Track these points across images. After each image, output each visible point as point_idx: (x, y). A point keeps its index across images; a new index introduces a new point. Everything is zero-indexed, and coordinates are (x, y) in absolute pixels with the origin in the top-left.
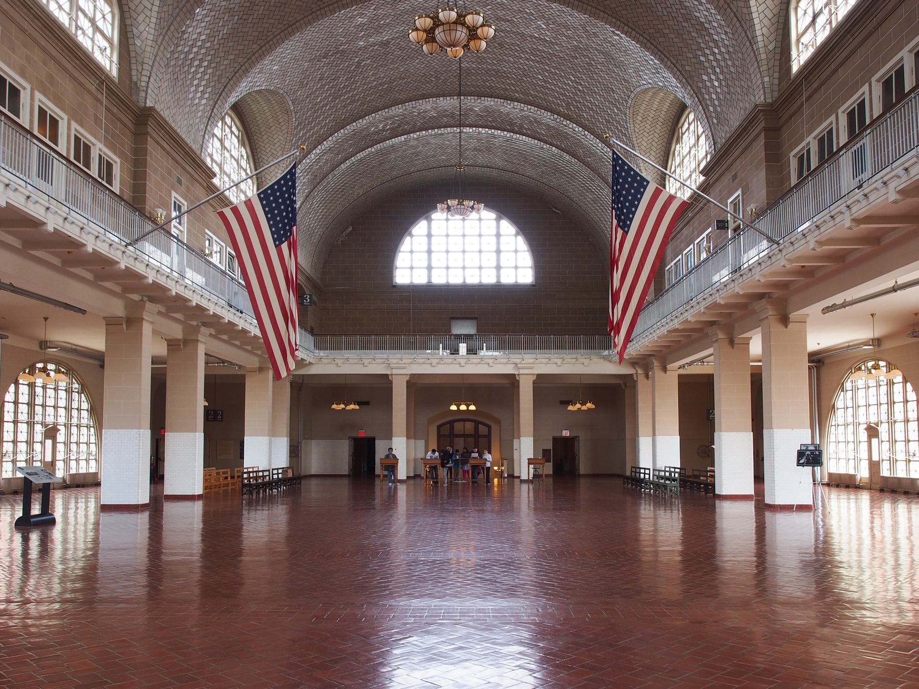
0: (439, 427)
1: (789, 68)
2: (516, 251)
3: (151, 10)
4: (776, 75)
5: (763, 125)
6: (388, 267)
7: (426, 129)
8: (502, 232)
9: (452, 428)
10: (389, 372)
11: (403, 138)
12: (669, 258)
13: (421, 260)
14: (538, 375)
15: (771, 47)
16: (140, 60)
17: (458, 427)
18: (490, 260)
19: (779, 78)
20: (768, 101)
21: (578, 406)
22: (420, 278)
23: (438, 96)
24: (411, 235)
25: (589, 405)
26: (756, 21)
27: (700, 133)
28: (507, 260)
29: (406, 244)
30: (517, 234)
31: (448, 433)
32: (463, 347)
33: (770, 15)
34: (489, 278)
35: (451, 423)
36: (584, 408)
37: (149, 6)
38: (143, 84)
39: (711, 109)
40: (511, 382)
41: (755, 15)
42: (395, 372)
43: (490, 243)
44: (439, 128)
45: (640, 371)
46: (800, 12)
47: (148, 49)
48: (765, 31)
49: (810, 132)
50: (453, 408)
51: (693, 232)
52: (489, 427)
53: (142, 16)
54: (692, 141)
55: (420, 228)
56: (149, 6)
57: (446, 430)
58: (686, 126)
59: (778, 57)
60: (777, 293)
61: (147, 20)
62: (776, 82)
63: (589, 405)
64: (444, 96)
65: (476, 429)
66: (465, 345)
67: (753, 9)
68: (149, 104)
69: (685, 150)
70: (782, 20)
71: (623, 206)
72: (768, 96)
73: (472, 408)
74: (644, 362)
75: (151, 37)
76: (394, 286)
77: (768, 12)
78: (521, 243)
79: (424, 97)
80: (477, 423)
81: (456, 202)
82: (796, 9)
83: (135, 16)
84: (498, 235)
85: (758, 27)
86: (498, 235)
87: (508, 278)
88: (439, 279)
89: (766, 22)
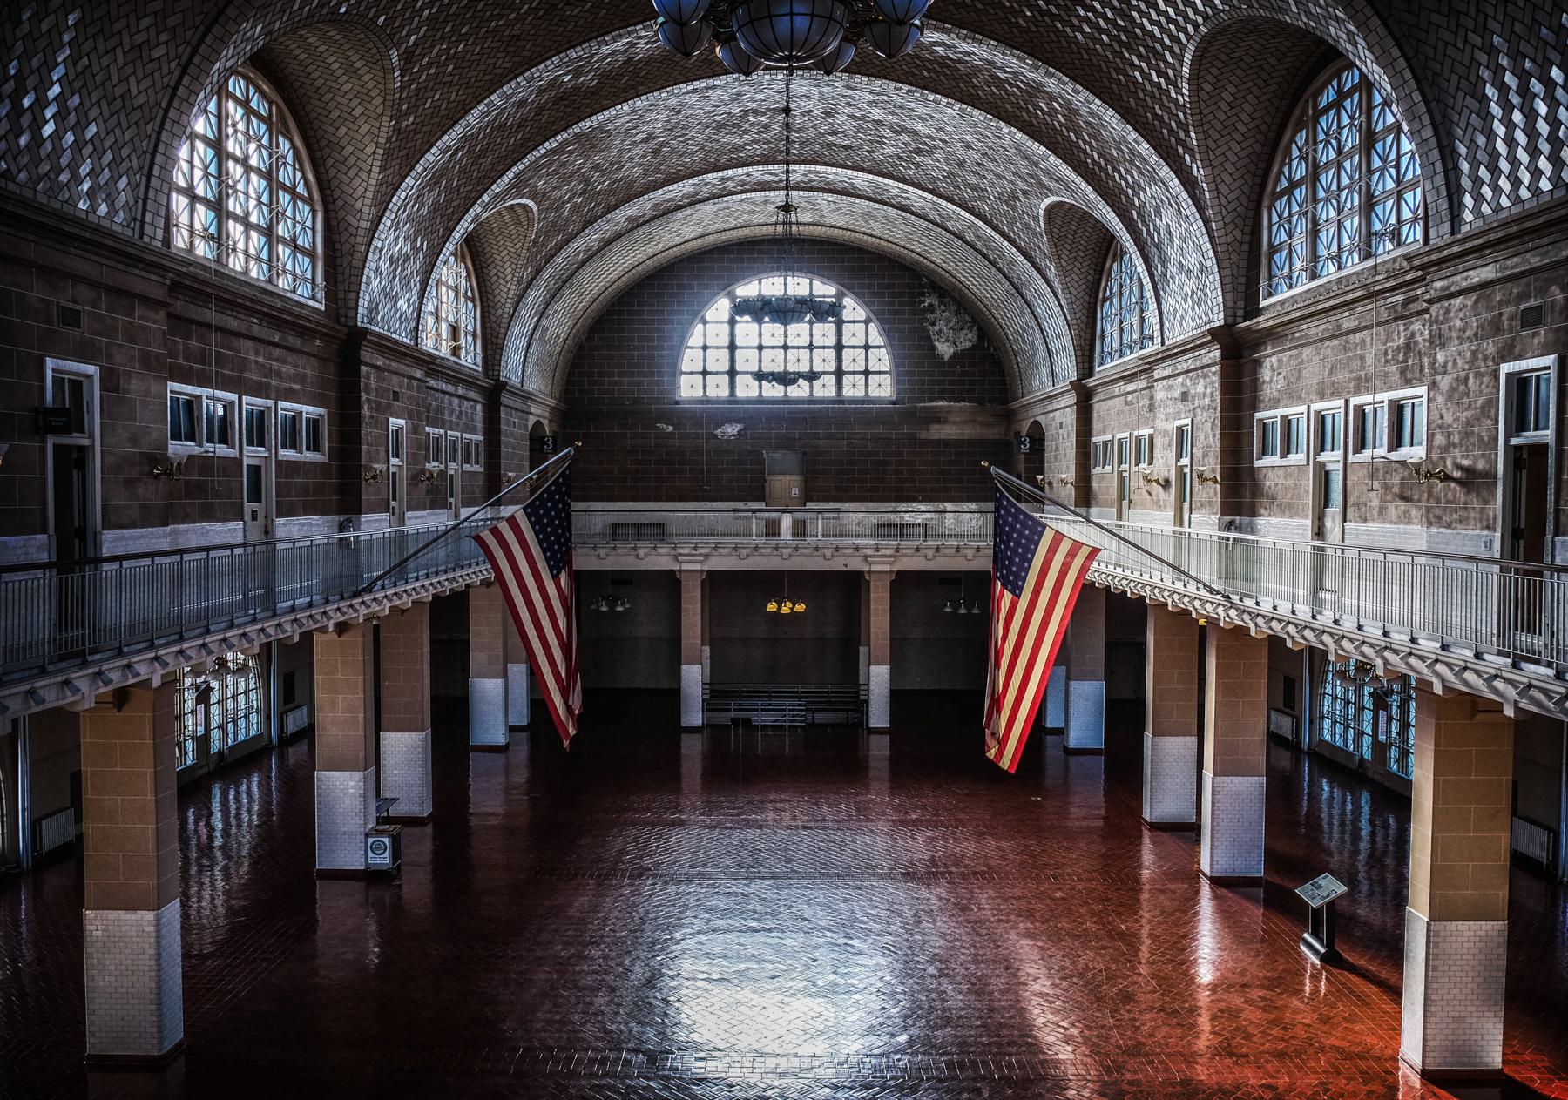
12: (1096, 425)
13: (718, 360)
18: (824, 360)
20: (1230, 320)
22: (718, 389)
24: (705, 322)
29: (696, 337)
30: (867, 322)
46: (1275, 219)
50: (772, 607)
55: (721, 308)
73: (800, 608)
76: (677, 403)
82: (1272, 205)
87: (853, 389)
88: (747, 389)
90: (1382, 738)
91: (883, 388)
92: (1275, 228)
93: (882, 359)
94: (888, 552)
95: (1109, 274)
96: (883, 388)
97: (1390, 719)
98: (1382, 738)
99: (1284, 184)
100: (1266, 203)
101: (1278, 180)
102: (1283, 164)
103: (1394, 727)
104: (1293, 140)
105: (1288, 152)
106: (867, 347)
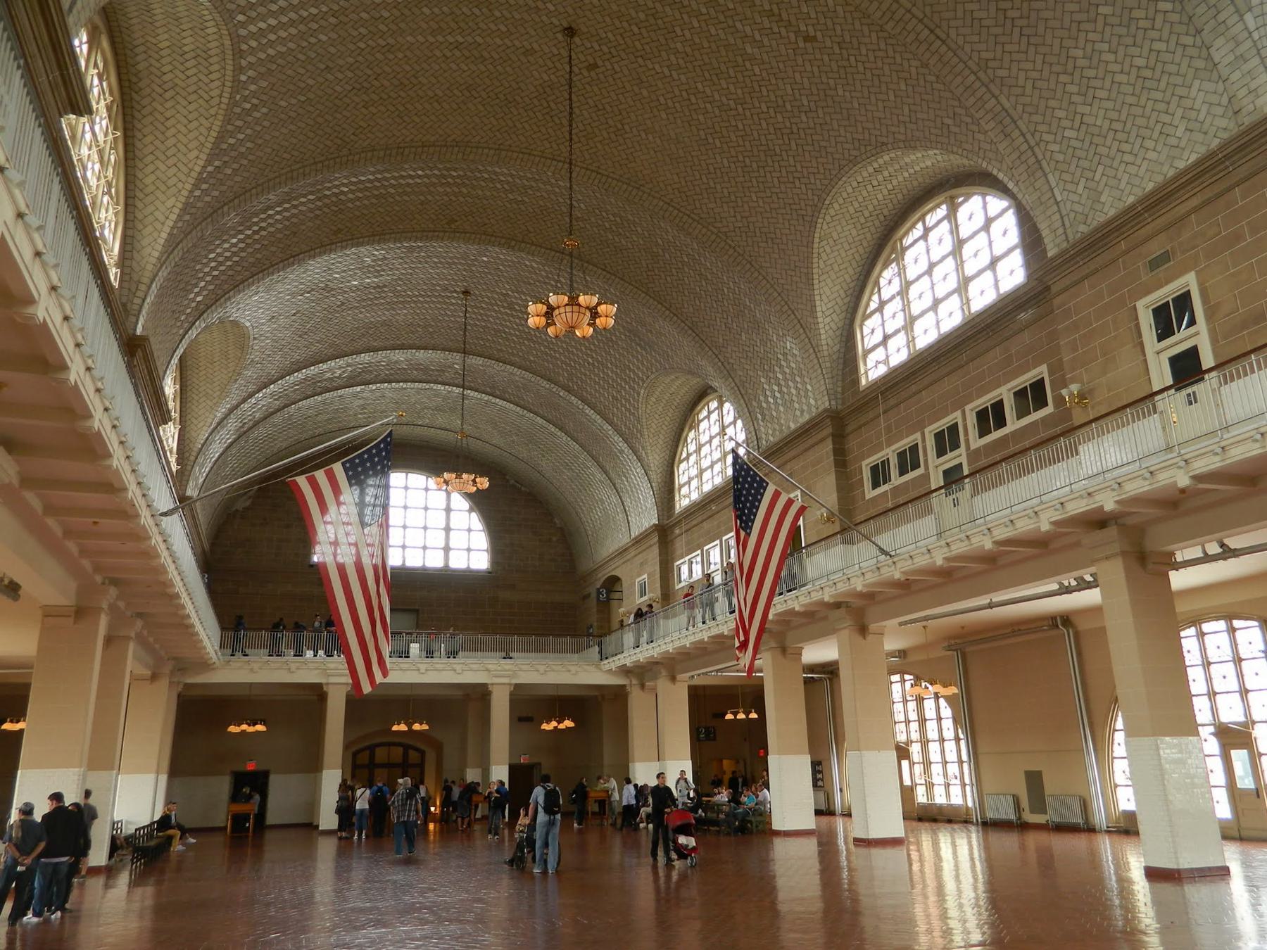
0: (355, 755)
1: (856, 381)
2: (469, 530)
3: (163, 224)
4: (840, 384)
5: (829, 430)
6: (306, 538)
7: (390, 382)
8: (452, 506)
9: (372, 756)
10: (323, 681)
11: (359, 389)
12: (678, 552)
14: (517, 686)
15: (835, 357)
16: (135, 277)
17: (381, 755)
18: (437, 539)
19: (843, 387)
21: (554, 724)
23: (418, 348)
25: (568, 723)
26: (822, 331)
27: (726, 423)
28: (457, 540)
30: (471, 510)
31: (367, 762)
32: (415, 648)
33: (834, 327)
34: (435, 561)
35: (372, 748)
36: (562, 726)
37: (162, 218)
38: (136, 307)
39: (754, 404)
40: (479, 695)
41: (821, 326)
42: (332, 680)
43: (438, 519)
44: (405, 381)
45: (635, 682)
46: (866, 330)
47: (150, 267)
48: (830, 341)
49: (889, 445)
51: (719, 527)
52: (423, 753)
53: (150, 228)
54: (716, 429)
56: (162, 218)
57: (364, 758)
58: (705, 413)
59: (841, 367)
60: (857, 603)
61: (155, 234)
62: (839, 389)
63: (568, 723)
64: (425, 348)
65: (405, 755)
66: (417, 645)
67: (820, 320)
68: (139, 331)
69: (704, 438)
70: (845, 333)
71: (744, 506)
72: (833, 403)
74: (643, 673)
75: (156, 254)
77: (833, 325)
78: (476, 521)
79: (402, 347)
80: (406, 748)
81: (454, 476)
83: (140, 226)
84: (448, 510)
85: (823, 337)
86: (448, 510)
87: (458, 562)
89: (831, 332)
90: (907, 782)
91: (481, 561)
92: (866, 340)
93: (481, 540)
94: (507, 667)
95: (686, 440)
96: (481, 561)
97: (912, 765)
98: (907, 782)
99: (873, 306)
100: (857, 322)
101: (868, 305)
102: (872, 294)
103: (918, 769)
104: (880, 275)
105: (877, 283)
106: (469, 530)
